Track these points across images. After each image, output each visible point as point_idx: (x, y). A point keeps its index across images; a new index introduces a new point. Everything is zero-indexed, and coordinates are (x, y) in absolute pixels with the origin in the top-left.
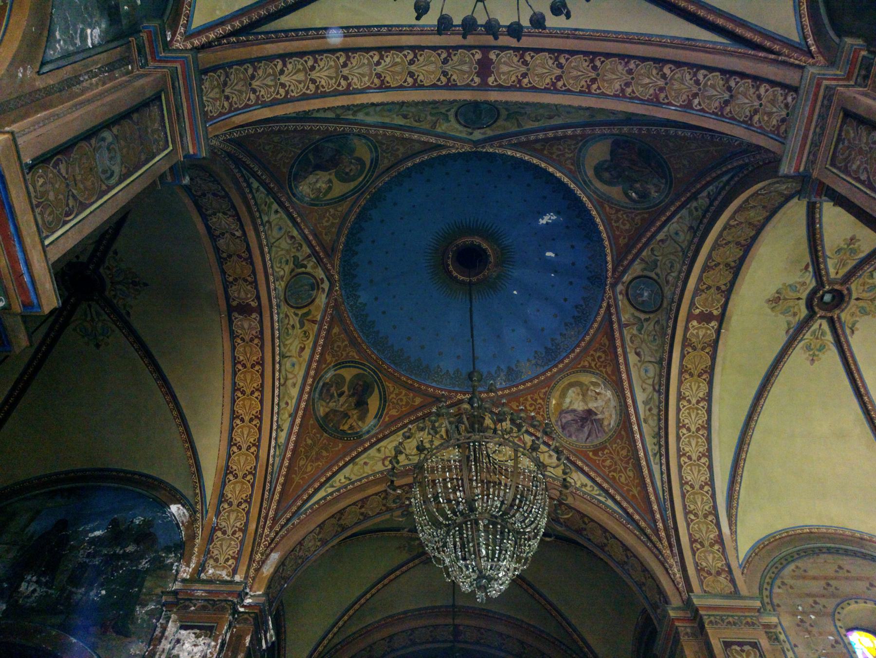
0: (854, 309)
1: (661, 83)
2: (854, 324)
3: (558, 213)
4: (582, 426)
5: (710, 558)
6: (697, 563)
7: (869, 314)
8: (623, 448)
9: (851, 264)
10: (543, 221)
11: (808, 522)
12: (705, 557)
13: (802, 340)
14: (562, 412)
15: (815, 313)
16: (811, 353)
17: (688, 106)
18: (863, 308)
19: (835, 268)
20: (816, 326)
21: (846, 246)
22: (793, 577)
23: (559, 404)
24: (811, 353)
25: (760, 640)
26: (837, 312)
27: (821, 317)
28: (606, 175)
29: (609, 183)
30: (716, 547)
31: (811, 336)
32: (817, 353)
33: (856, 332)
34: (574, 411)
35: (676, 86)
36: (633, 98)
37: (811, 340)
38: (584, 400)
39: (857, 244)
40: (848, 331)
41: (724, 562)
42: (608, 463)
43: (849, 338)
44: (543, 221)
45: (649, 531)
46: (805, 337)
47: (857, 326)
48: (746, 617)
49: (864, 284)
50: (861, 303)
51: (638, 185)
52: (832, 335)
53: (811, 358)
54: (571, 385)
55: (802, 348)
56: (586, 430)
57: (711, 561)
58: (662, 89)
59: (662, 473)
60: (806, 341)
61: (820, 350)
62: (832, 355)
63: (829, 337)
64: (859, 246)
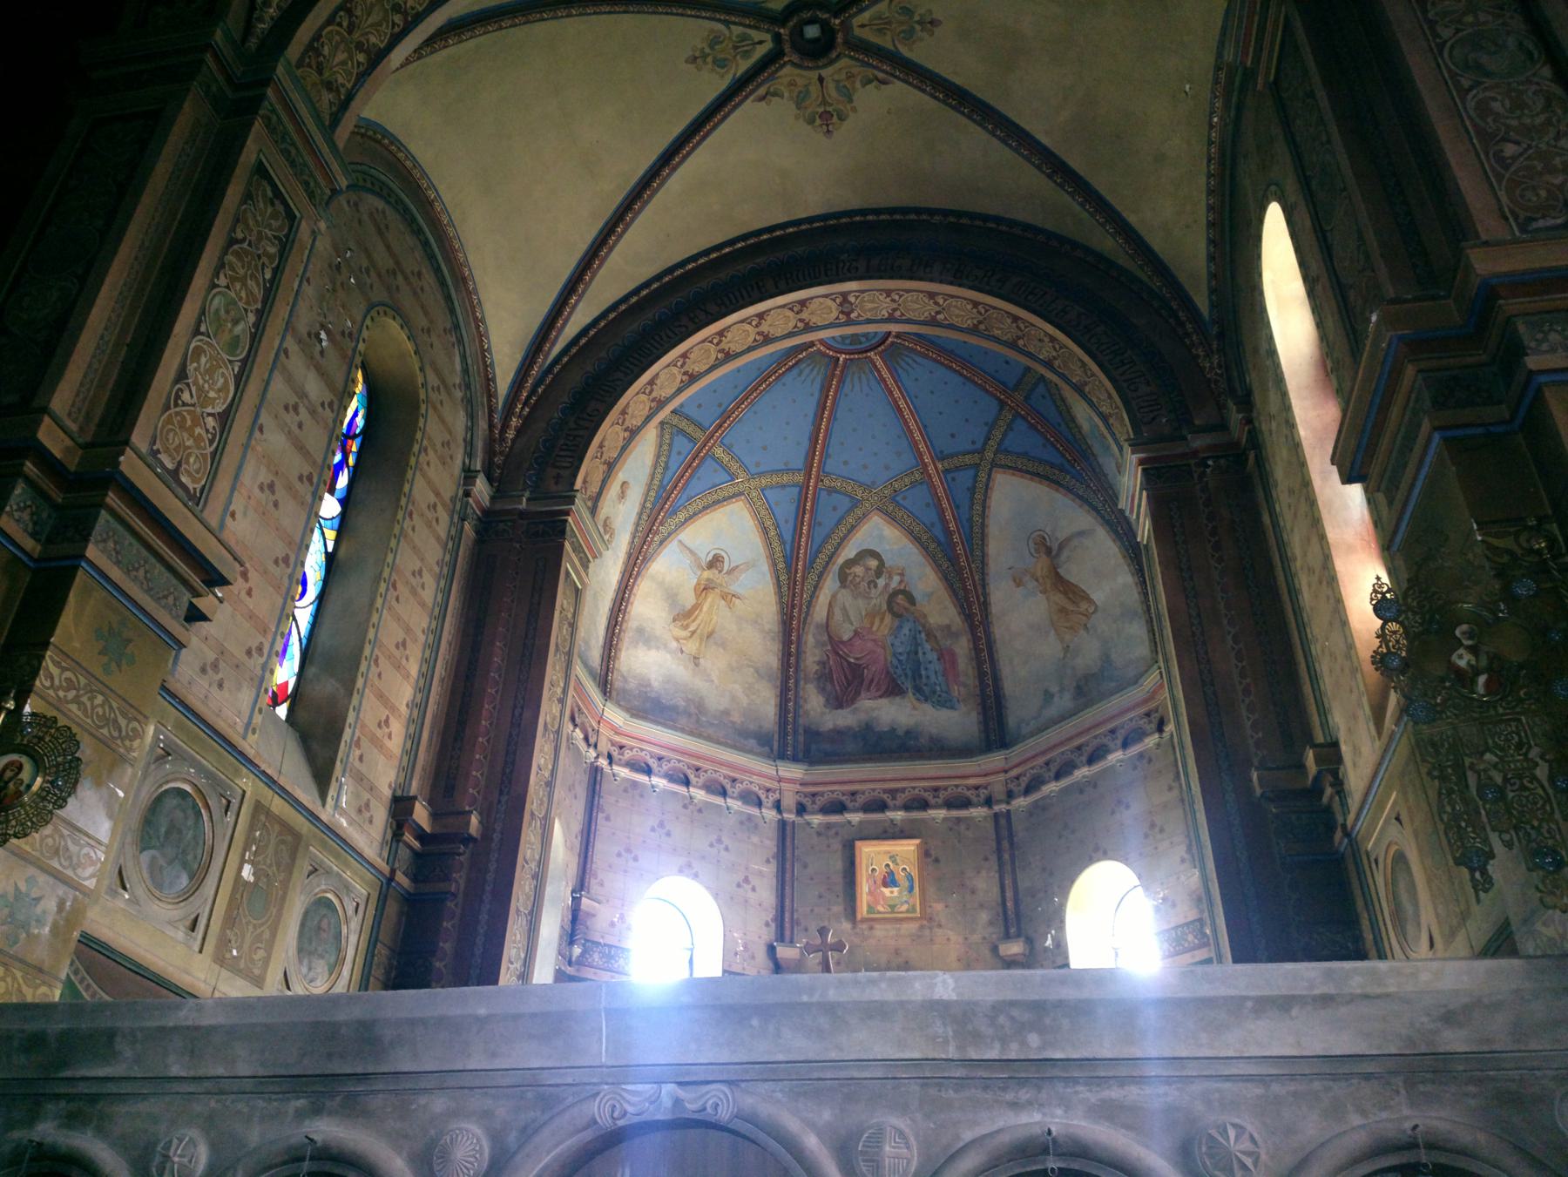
0: (800, 82)
2: (775, 94)
5: (341, 56)
6: (320, 36)
7: (799, 109)
9: (885, 42)
11: (441, 189)
12: (337, 48)
13: (727, 23)
15: (783, 25)
16: (707, 50)
18: (808, 92)
19: (871, 19)
20: (756, 35)
21: (917, 18)
22: (371, 215)
24: (707, 50)
25: (303, 223)
26: (795, 58)
27: (777, 38)
30: (361, 57)
31: (738, 36)
32: (709, 59)
33: (763, 103)
37: (730, 38)
39: (925, 35)
40: (762, 91)
41: (349, 86)
43: (752, 98)
46: (733, 27)
47: (775, 99)
48: (311, 175)
49: (850, 76)
50: (814, 89)
52: (747, 72)
53: (697, 54)
55: (712, 31)
57: (337, 60)
60: (727, 32)
61: (715, 61)
62: (713, 85)
63: (743, 66)
64: (921, 39)
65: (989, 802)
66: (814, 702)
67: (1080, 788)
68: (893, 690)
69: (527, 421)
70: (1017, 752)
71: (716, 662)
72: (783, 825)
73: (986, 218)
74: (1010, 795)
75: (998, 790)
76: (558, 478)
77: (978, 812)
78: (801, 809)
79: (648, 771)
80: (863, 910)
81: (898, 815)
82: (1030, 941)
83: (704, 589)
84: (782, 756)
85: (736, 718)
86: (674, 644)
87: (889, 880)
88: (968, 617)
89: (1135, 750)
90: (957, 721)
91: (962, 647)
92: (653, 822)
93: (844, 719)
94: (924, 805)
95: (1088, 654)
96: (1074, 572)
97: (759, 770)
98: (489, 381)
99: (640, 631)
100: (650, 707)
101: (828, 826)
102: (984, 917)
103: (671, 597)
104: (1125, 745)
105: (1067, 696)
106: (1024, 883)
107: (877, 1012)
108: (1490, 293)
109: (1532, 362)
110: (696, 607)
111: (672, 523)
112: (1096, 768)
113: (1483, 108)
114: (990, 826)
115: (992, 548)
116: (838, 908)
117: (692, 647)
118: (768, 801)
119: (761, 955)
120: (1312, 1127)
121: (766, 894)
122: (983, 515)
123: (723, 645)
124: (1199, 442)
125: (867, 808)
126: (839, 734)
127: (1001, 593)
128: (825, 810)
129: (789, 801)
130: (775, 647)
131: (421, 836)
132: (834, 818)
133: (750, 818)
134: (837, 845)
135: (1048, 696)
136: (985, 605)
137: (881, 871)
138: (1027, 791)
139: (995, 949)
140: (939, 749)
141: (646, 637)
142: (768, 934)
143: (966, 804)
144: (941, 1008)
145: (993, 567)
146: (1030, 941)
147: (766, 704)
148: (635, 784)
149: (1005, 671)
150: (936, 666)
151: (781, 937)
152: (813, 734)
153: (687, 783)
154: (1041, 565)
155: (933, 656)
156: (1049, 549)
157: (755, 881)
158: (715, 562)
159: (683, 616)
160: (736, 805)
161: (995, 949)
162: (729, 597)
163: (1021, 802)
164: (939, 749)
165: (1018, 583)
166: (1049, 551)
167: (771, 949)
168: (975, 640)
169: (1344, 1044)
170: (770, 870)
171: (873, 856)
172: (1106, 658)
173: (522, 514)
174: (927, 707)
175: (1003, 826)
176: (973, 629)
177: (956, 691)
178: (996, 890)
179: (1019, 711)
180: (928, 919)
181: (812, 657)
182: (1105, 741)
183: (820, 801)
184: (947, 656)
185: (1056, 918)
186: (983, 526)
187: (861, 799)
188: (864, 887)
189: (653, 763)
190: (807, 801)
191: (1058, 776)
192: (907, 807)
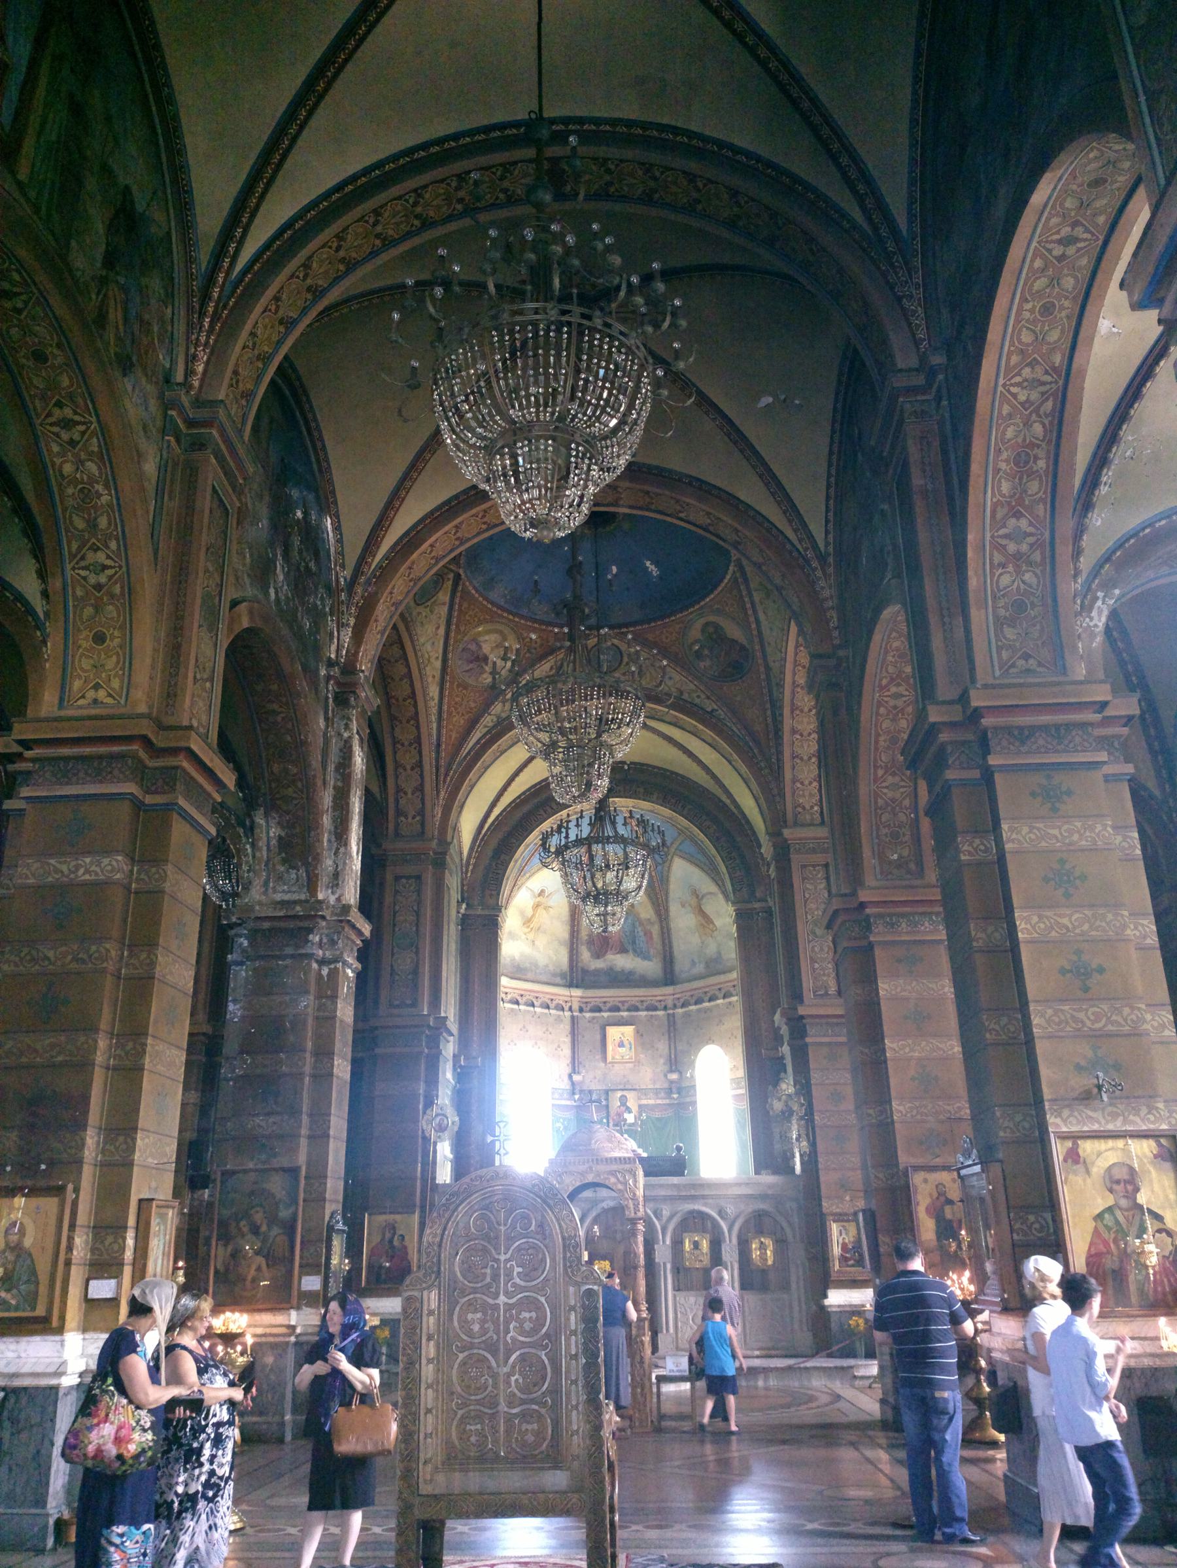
1: (806, 709)
3: (660, 577)
4: (471, 662)
8: (475, 702)
10: (648, 564)
14: (474, 640)
17: (794, 731)
23: (480, 634)
28: (711, 630)
29: (703, 631)
34: (480, 647)
35: (805, 720)
36: (793, 693)
38: (492, 649)
42: (457, 699)
44: (648, 564)
45: (442, 770)
51: (706, 652)
54: (501, 632)
56: (471, 666)
58: (802, 711)
59: (478, 742)
65: (665, 1008)
66: (585, 955)
67: (706, 1010)
68: (623, 950)
69: (475, 865)
70: (679, 988)
71: (542, 941)
72: (573, 1017)
73: (677, 774)
74: (675, 1006)
75: (670, 1003)
76: (491, 895)
77: (661, 1013)
78: (581, 1010)
79: (517, 1003)
80: (609, 1059)
81: (625, 1014)
82: (681, 1073)
83: (537, 906)
84: (570, 985)
85: (551, 968)
86: (524, 937)
87: (621, 1045)
88: (658, 913)
89: (727, 1000)
90: (651, 967)
91: (655, 930)
92: (521, 1026)
93: (599, 964)
94: (637, 1009)
95: (711, 949)
96: (708, 908)
97: (562, 993)
98: (461, 853)
99: (510, 933)
100: (519, 973)
101: (594, 1018)
102: (662, 1061)
103: (522, 913)
104: (724, 997)
105: (702, 966)
106: (680, 1048)
107: (661, 1186)
108: (802, 1017)
109: (808, 1040)
110: (533, 916)
111: (523, 879)
112: (712, 1003)
113: (813, 950)
114: (665, 1019)
115: (672, 887)
116: (598, 1057)
117: (531, 936)
118: (566, 1008)
119: (566, 1078)
120: (742, 1207)
121: (567, 1051)
122: (669, 871)
123: (545, 932)
124: (757, 905)
125: (610, 1010)
126: (597, 972)
127: (674, 908)
128: (592, 1011)
129: (576, 1006)
130: (568, 928)
131: (461, 1067)
132: (597, 1014)
133: (559, 1016)
134: (597, 1027)
135: (693, 963)
136: (667, 910)
137: (618, 1040)
138: (683, 1006)
139: (666, 1076)
140: (643, 982)
141: (512, 936)
142: (568, 1070)
143: (655, 1009)
144: (675, 1185)
145: (671, 895)
146: (681, 1073)
147: (563, 957)
148: (512, 1010)
149: (675, 944)
150: (643, 938)
151: (574, 1071)
152: (585, 972)
153: (533, 1005)
154: (694, 902)
155: (642, 934)
156: (698, 897)
157: (562, 1046)
158: (542, 893)
159: (527, 922)
160: (553, 1012)
161: (666, 1076)
162: (547, 908)
163: (680, 1011)
164: (643, 982)
165: (683, 906)
166: (697, 897)
167: (570, 1076)
168: (662, 928)
169: (750, 1192)
170: (568, 1040)
171: (614, 1033)
172: (719, 953)
173: (479, 916)
174: (638, 960)
175: (671, 1020)
176: (661, 922)
177: (652, 951)
178: (667, 1051)
179: (682, 965)
180: (637, 1062)
181: (584, 934)
182: (717, 993)
183: (589, 1006)
184: (648, 934)
185: (692, 1064)
186: (668, 877)
187: (608, 1005)
188: (610, 1048)
189: (519, 998)
190: (583, 1006)
191: (696, 1003)
192: (629, 1010)
